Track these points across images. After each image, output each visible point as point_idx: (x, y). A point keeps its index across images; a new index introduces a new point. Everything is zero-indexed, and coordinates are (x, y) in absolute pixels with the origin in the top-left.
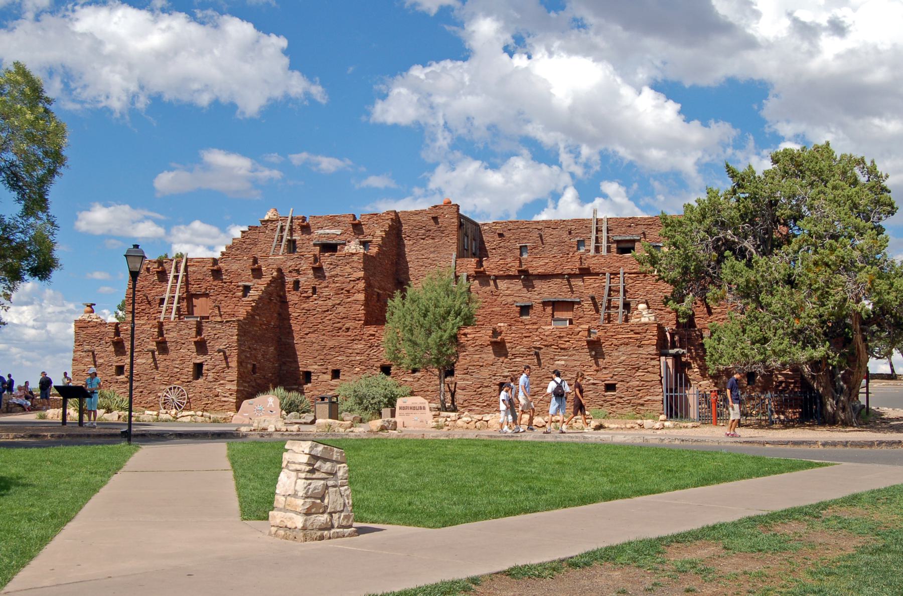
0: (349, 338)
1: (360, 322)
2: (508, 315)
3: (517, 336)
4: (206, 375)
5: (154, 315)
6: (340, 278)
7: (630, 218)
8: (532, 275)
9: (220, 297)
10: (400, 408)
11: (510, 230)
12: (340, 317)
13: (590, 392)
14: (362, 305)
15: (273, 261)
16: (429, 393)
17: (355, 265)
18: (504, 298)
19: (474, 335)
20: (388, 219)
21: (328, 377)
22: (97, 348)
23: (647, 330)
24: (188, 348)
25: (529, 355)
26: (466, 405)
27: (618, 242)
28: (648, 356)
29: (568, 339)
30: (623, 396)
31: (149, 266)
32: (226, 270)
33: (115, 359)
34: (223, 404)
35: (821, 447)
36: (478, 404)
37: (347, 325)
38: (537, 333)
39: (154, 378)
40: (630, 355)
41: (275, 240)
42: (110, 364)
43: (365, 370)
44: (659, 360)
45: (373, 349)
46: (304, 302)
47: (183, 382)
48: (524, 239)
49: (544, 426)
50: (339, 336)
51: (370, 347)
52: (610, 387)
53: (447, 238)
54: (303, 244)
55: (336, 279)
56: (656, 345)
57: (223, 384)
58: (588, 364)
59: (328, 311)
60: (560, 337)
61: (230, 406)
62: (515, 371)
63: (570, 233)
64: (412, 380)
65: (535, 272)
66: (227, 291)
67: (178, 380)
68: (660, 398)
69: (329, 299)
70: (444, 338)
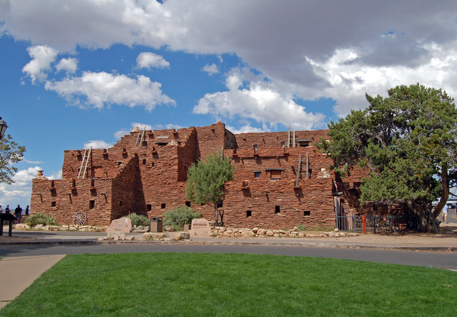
0: (170, 188)
1: (175, 180)
2: (249, 176)
3: (256, 185)
4: (96, 206)
5: (75, 177)
7: (306, 131)
8: (260, 157)
9: (107, 168)
10: (194, 225)
11: (249, 137)
12: (165, 177)
13: (296, 216)
14: (177, 171)
15: (133, 150)
16: (210, 215)
17: (173, 152)
18: (247, 168)
19: (233, 185)
20: (190, 131)
21: (159, 207)
22: (43, 193)
23: (327, 182)
25: (263, 196)
26: (229, 223)
27: (300, 142)
28: (327, 196)
29: (283, 187)
30: (314, 218)
31: (74, 153)
32: (110, 155)
34: (104, 221)
35: (450, 251)
36: (235, 222)
37: (169, 182)
38: (267, 184)
39: (70, 208)
40: (318, 195)
41: (137, 142)
42: (49, 201)
43: (178, 204)
44: (334, 199)
45: (182, 194)
46: (148, 170)
47: (84, 210)
48: (256, 141)
49: (273, 235)
50: (165, 187)
51: (180, 192)
52: (307, 213)
53: (219, 140)
54: (150, 143)
56: (332, 190)
57: (104, 211)
58: (295, 201)
59: (160, 174)
60: (279, 186)
61: (107, 223)
62: (255, 204)
63: (277, 138)
64: (201, 209)
65: (262, 156)
66: (111, 165)
67: (82, 209)
68: (334, 219)
69: (160, 168)
70: (217, 187)
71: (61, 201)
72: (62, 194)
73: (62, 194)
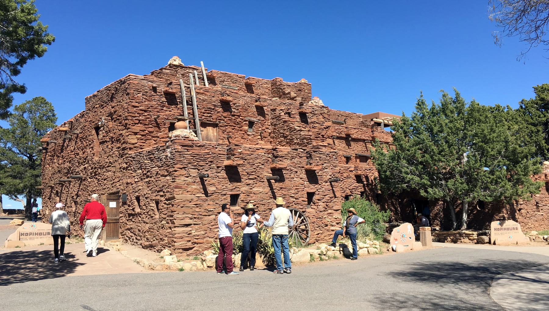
6: (317, 125)
10: (495, 229)
32: (234, 104)
33: (230, 186)
42: (224, 193)
55: (315, 125)
66: (235, 123)
72: (251, 177)
73: (251, 177)
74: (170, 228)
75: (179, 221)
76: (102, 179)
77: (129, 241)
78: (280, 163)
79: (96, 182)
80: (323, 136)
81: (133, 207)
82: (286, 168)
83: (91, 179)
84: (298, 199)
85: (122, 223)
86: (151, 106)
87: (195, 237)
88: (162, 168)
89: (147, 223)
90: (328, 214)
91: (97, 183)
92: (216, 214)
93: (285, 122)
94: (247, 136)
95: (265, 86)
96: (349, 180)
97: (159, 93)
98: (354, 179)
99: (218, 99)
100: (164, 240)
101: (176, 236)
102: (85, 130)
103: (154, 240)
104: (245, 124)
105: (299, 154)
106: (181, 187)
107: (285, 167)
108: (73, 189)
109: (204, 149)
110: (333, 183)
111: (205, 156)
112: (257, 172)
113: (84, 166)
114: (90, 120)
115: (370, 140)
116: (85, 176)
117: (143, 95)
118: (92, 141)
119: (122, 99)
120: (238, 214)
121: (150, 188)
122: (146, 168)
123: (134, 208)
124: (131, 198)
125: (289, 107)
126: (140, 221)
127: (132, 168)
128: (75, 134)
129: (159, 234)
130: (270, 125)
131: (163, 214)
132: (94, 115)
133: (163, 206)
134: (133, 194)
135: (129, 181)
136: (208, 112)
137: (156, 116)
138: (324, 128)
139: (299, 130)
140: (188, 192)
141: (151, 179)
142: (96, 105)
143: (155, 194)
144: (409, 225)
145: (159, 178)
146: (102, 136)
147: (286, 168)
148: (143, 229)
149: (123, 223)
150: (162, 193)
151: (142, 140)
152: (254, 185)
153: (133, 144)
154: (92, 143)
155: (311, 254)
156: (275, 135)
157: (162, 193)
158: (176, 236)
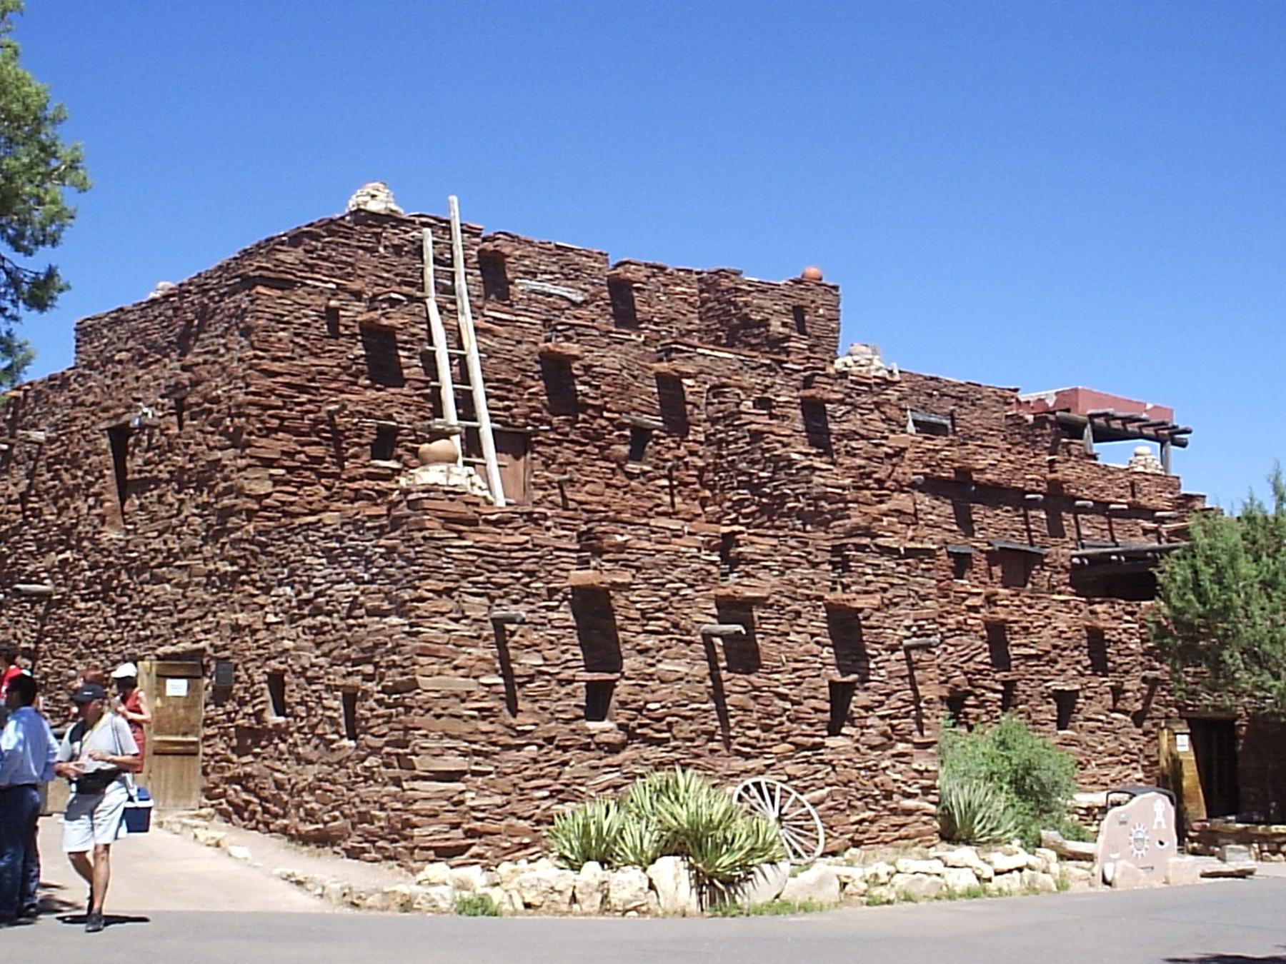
7: (932, 379)
15: (707, 362)
24: (810, 629)
31: (333, 303)
34: (902, 819)
42: (566, 674)
55: (854, 444)
66: (584, 435)
71: (650, 677)
74: (397, 782)
75: (428, 758)
76: (134, 606)
77: (235, 817)
78: (746, 581)
79: (109, 612)
80: (877, 481)
81: (260, 707)
82: (767, 598)
83: (87, 601)
84: (800, 704)
85: (212, 756)
86: (321, 373)
87: (474, 814)
88: (373, 587)
89: (311, 762)
90: (894, 756)
91: (113, 616)
92: (540, 742)
93: (757, 436)
94: (623, 478)
95: (678, 289)
96: (964, 638)
97: (347, 327)
98: (982, 638)
99: (534, 348)
100: (374, 817)
101: (415, 807)
102: (72, 433)
103: (335, 819)
104: (619, 436)
105: (810, 553)
106: (438, 650)
107: (764, 595)
108: (11, 631)
109: (510, 531)
110: (915, 655)
111: (513, 555)
112: (670, 610)
113: (61, 557)
114: (91, 398)
115: (1040, 493)
116: (63, 589)
117: (297, 335)
118: (97, 474)
119: (225, 345)
120: (607, 744)
121: (325, 648)
122: (310, 583)
123: (262, 710)
124: (250, 676)
125: (768, 381)
126: (282, 753)
127: (256, 577)
128: (31, 442)
129: (357, 800)
130: (701, 443)
131: (373, 735)
132: (108, 386)
133: (372, 710)
134: (258, 664)
135: (243, 618)
136: (498, 392)
137: (333, 407)
138: (887, 455)
139: (804, 468)
140: (456, 668)
141: (328, 620)
142: (120, 351)
143: (343, 670)
144: (1159, 801)
145: (362, 617)
146: (140, 461)
147: (767, 598)
148: (293, 781)
149: (217, 758)
150: (369, 669)
151: (287, 483)
152: (662, 653)
153: (259, 498)
154: (97, 479)
155: (845, 880)
156: (721, 479)
157: (369, 669)
158: (415, 807)
